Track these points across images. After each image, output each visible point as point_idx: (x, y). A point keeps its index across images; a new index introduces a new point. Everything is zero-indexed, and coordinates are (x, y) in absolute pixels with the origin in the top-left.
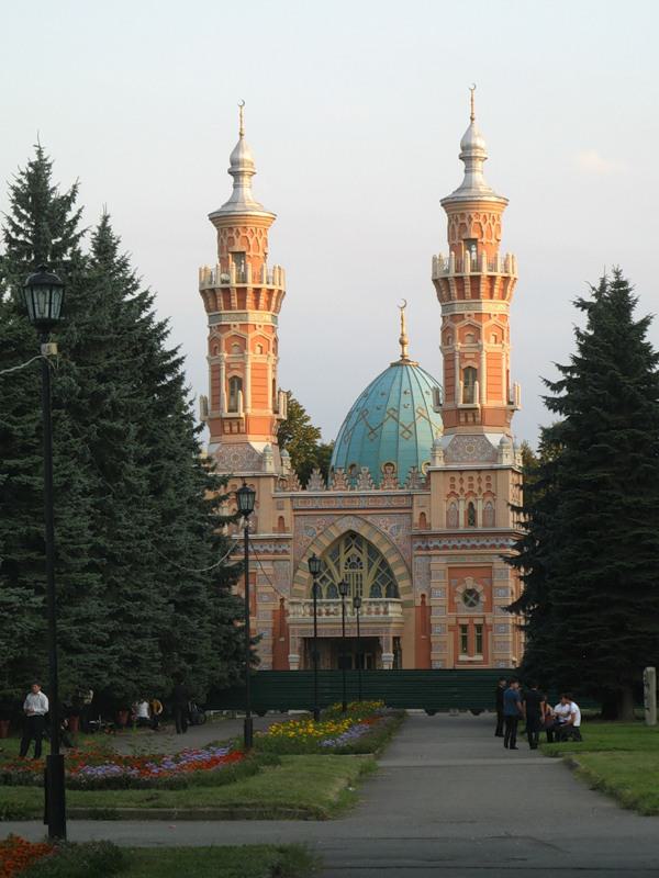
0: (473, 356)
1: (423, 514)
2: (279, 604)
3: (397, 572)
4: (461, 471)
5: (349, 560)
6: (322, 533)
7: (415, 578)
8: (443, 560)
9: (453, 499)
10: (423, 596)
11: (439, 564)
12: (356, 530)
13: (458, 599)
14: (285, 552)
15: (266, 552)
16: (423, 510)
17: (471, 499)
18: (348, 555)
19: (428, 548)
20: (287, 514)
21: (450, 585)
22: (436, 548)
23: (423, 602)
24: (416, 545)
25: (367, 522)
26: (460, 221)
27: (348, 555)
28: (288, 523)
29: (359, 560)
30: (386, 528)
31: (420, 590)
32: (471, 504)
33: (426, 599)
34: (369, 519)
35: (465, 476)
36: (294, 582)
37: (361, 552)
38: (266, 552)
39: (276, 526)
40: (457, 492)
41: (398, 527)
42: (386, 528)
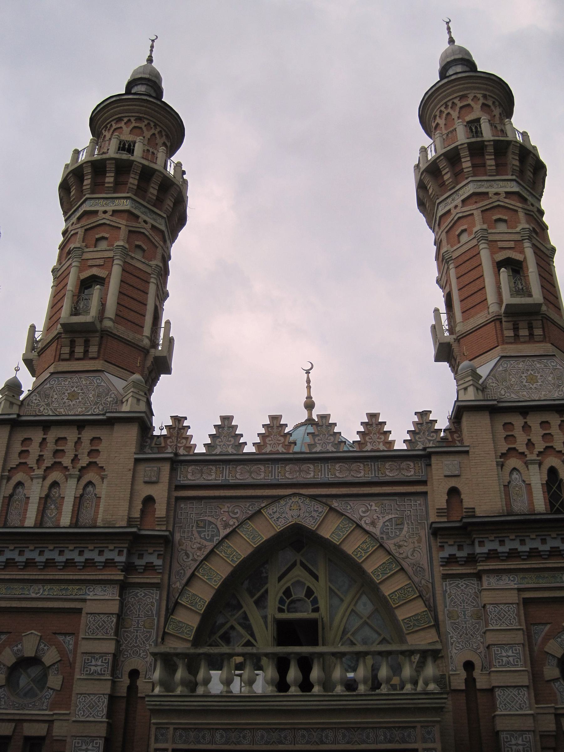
0: (512, 244)
1: (454, 492)
2: (125, 681)
3: (402, 615)
4: (524, 411)
5: (287, 593)
6: (234, 531)
7: (447, 626)
8: (508, 582)
9: (513, 462)
10: (469, 666)
11: (502, 592)
12: (310, 524)
13: (551, 671)
14: (149, 567)
15: (109, 564)
16: (453, 483)
17: (552, 461)
18: (287, 582)
19: (472, 559)
20: (160, 493)
21: (529, 636)
22: (492, 555)
23: (470, 681)
24: (445, 554)
25: (332, 509)
26: (460, 104)
27: (287, 582)
28: (161, 509)
29: (309, 593)
30: (373, 524)
31: (457, 655)
32: (553, 472)
33: (477, 673)
34: (335, 504)
35: (534, 421)
36: (165, 633)
37: (316, 578)
38: (109, 564)
39: (137, 514)
40: (522, 448)
41: (399, 523)
42: (373, 524)
